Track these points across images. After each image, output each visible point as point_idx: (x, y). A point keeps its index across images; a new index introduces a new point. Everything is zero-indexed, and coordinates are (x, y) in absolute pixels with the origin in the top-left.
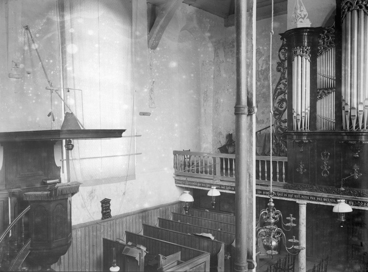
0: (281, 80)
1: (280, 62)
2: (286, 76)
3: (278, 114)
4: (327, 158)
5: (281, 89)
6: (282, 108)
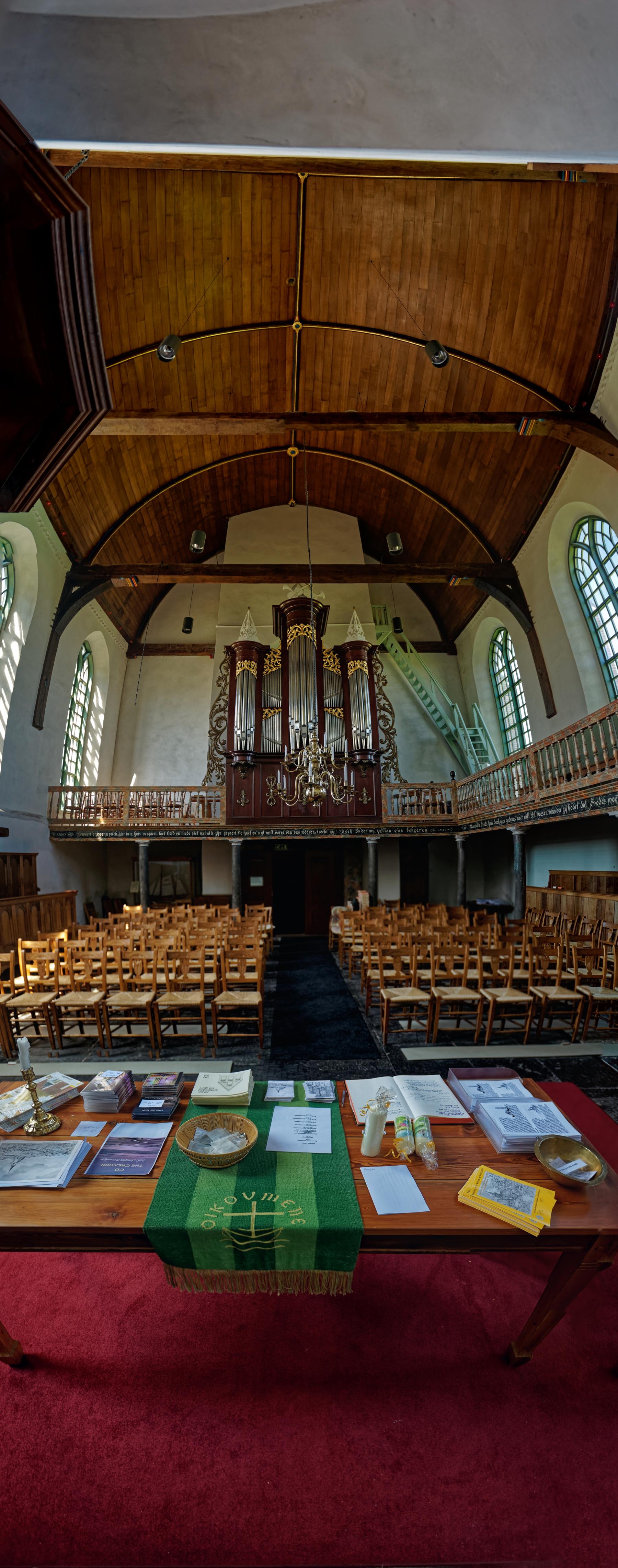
3: (214, 735)
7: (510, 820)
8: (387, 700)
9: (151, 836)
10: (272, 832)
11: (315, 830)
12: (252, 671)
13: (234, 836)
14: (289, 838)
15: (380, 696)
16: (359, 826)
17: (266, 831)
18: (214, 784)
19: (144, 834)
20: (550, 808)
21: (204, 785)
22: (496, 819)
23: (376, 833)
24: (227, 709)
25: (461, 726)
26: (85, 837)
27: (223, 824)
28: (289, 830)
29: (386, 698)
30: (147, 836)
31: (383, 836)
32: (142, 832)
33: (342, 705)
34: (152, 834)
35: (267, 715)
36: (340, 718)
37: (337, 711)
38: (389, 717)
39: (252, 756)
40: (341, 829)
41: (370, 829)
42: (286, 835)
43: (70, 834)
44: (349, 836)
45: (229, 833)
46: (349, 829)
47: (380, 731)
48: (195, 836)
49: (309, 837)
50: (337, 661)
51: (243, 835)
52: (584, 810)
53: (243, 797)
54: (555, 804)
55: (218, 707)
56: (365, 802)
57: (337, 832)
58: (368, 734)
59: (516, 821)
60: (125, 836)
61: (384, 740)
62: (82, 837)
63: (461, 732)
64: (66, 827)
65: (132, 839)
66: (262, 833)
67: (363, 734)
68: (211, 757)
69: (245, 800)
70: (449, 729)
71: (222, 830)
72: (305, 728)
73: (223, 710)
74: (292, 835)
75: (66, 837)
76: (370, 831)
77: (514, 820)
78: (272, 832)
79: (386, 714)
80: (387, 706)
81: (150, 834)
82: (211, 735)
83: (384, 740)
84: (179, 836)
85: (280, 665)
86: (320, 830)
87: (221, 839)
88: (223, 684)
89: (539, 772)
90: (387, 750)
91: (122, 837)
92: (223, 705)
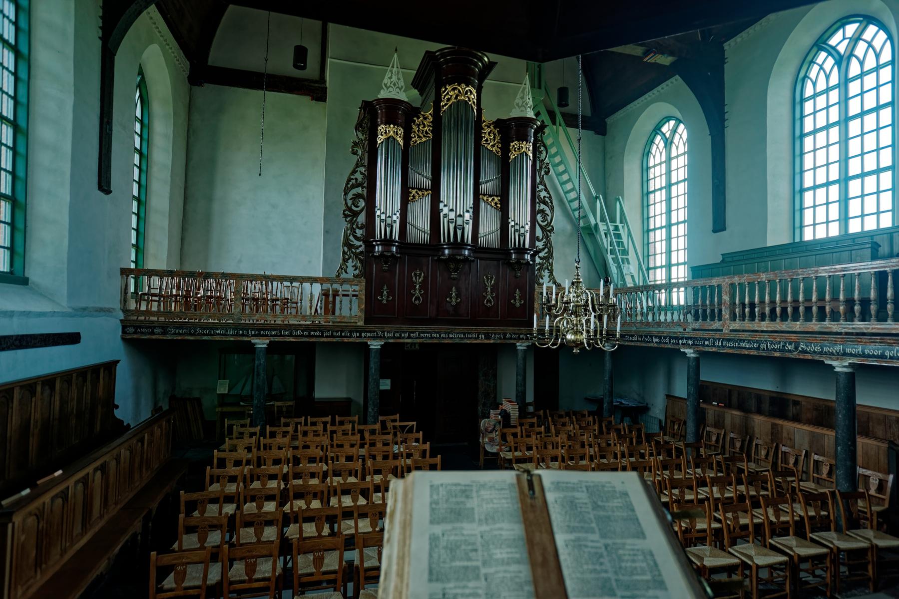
0: (357, 166)
2: (366, 162)
3: (349, 216)
4: (419, 279)
5: (356, 179)
6: (358, 207)
7: (685, 341)
8: (548, 193)
9: (272, 336)
10: (416, 334)
14: (435, 341)
15: (541, 187)
18: (350, 276)
20: (744, 341)
21: (338, 276)
22: (665, 337)
24: (365, 185)
25: (603, 220)
26: (180, 334)
27: (361, 323)
28: (436, 333)
29: (546, 190)
30: (266, 336)
32: (260, 330)
33: (499, 193)
34: (273, 333)
35: (414, 196)
36: (497, 208)
37: (493, 199)
38: (548, 212)
39: (396, 246)
40: (492, 334)
41: (521, 334)
42: (432, 338)
43: (157, 330)
44: (499, 342)
45: (369, 335)
46: (500, 334)
48: (327, 337)
49: (457, 341)
50: (498, 138)
51: (384, 337)
52: (789, 351)
54: (750, 338)
55: (354, 181)
56: (518, 305)
57: (488, 337)
59: (693, 344)
60: (237, 335)
61: (541, 238)
62: (175, 334)
63: (602, 227)
64: (153, 322)
66: (406, 335)
67: (522, 231)
68: (347, 243)
69: (388, 297)
70: (589, 221)
71: (360, 330)
74: (439, 338)
75: (153, 333)
76: (521, 336)
77: (691, 342)
78: (416, 334)
79: (546, 208)
80: (547, 199)
81: (270, 333)
82: (346, 216)
83: (541, 238)
84: (306, 336)
85: (431, 135)
86: (469, 333)
88: (360, 152)
89: (733, 304)
90: (543, 249)
92: (360, 180)
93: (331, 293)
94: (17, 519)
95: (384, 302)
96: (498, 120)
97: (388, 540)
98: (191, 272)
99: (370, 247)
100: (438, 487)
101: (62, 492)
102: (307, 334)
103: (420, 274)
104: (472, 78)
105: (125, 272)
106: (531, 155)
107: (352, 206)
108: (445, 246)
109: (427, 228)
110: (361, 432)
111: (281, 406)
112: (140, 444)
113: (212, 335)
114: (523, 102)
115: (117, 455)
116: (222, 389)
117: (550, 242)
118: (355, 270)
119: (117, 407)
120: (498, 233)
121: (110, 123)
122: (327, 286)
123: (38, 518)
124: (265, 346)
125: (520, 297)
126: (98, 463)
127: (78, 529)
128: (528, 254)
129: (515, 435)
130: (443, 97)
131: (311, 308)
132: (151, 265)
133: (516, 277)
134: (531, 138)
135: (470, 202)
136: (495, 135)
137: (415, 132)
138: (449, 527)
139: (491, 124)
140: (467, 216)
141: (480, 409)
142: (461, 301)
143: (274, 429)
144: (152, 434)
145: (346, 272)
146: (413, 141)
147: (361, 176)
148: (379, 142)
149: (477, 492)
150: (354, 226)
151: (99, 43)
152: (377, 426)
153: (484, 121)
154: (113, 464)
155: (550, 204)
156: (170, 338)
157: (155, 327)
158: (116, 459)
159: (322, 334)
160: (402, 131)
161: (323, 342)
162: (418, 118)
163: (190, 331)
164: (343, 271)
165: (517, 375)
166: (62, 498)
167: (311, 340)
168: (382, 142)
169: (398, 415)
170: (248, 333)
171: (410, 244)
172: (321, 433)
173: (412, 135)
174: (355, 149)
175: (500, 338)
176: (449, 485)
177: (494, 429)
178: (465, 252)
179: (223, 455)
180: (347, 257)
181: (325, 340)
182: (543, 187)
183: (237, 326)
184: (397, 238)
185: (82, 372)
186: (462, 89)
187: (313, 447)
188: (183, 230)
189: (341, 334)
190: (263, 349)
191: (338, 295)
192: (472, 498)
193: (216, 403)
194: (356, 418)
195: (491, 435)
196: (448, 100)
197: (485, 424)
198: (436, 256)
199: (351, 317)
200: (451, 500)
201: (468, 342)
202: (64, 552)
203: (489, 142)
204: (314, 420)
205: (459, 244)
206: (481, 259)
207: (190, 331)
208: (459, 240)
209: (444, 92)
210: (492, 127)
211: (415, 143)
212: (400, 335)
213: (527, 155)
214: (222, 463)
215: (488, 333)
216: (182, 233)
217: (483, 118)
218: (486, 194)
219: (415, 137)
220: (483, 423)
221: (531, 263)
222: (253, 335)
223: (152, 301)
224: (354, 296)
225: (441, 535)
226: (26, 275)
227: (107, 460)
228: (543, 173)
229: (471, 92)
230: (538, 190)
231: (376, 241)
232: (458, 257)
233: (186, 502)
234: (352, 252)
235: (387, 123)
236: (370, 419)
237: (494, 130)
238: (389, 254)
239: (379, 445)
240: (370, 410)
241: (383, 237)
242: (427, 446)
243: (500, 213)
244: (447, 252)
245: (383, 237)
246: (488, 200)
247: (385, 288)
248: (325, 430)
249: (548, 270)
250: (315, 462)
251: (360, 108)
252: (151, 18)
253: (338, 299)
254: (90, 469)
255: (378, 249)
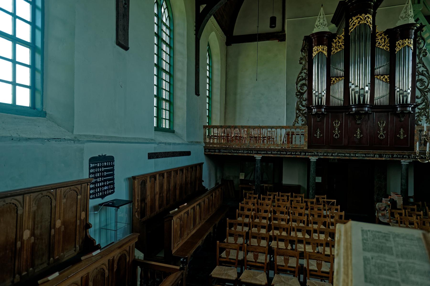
0: (302, 70)
1: (302, 57)
2: (307, 67)
3: (299, 95)
4: (338, 125)
5: (302, 76)
8: (426, 68)
9: (263, 154)
10: (336, 154)
11: (365, 154)
12: (324, 52)
13: (313, 156)
14: (347, 158)
15: (419, 65)
16: (396, 153)
17: (332, 153)
19: (259, 152)
21: (294, 125)
23: (409, 158)
24: (307, 79)
26: (225, 152)
27: (306, 148)
28: (348, 153)
29: (424, 66)
30: (261, 154)
31: (414, 160)
32: (258, 151)
33: (388, 72)
34: (263, 152)
35: (334, 81)
37: (384, 77)
39: (324, 108)
41: (404, 155)
42: (345, 156)
43: (217, 151)
44: (388, 159)
45: (310, 154)
46: (389, 154)
47: (417, 89)
48: (289, 154)
49: (361, 158)
50: (387, 40)
51: (318, 155)
53: (318, 133)
55: (301, 78)
57: (380, 156)
58: (409, 93)
60: (248, 153)
62: (223, 152)
64: (215, 147)
65: (252, 155)
66: (330, 154)
67: (405, 93)
68: (298, 109)
69: (320, 135)
72: (363, 90)
73: (304, 79)
74: (350, 156)
75: (215, 152)
76: (405, 156)
78: (336, 154)
80: (424, 72)
81: (262, 152)
82: (297, 95)
83: (419, 96)
85: (343, 47)
87: (304, 157)
88: (304, 63)
90: (421, 103)
91: (246, 153)
92: (304, 76)
93: (290, 133)
94: (174, 218)
95: (318, 137)
96: (387, 30)
97: (338, 255)
98: (229, 126)
99: (310, 109)
100: (366, 231)
101: (187, 211)
102: (279, 153)
103: (338, 122)
104: (369, 9)
105: (205, 127)
106: (412, 46)
107: (301, 90)
108: (353, 106)
109: (342, 97)
110: (306, 202)
111: (267, 186)
112: (211, 197)
113: (238, 153)
114: (406, 15)
115: (204, 200)
116: (242, 177)
117: (427, 99)
118: (302, 122)
119: (203, 181)
120: (388, 96)
121: (198, 68)
122: (288, 130)
123: (180, 220)
124: (260, 158)
125: (403, 133)
126: (198, 202)
127: (192, 227)
128: (410, 107)
129: (401, 214)
130: (350, 24)
131: (281, 141)
132: (214, 123)
133: (400, 121)
134: (412, 35)
135: (368, 80)
136: (385, 39)
137: (334, 47)
138: (376, 255)
139: (382, 34)
140: (367, 88)
141: (375, 197)
142: (363, 136)
143: (264, 196)
144: (216, 193)
145: (298, 123)
146: (333, 52)
147: (305, 75)
148: (314, 55)
149: (394, 238)
150: (301, 100)
151: (195, 36)
152: (315, 200)
153: (378, 33)
154: (203, 203)
155: (427, 75)
156: (221, 154)
157: (216, 149)
158: (203, 202)
159: (286, 153)
160: (326, 47)
161: (287, 157)
162: (336, 39)
163: (229, 151)
164: (296, 122)
165: (401, 179)
166: (187, 214)
167: (281, 156)
168: (316, 55)
169: (326, 196)
170: (253, 152)
171: (332, 107)
172: (286, 200)
173: (332, 49)
174: (301, 61)
175: (389, 157)
176: (374, 231)
177: (385, 209)
178: (365, 109)
179: (243, 205)
180: (298, 115)
181: (288, 156)
182: (421, 65)
183: (248, 149)
184: (325, 104)
185: (192, 167)
186: (363, 17)
187: (282, 207)
188: (226, 108)
189: (296, 153)
190: (259, 160)
191: (294, 135)
192: (390, 241)
193: (239, 183)
194: (303, 195)
195: (383, 212)
196: (354, 25)
197: (379, 206)
198: (347, 112)
199: (300, 145)
200: (376, 240)
201: (368, 159)
202: (188, 234)
203: (381, 44)
204: (283, 194)
205: (362, 104)
206: (376, 112)
207: (229, 151)
208: (362, 102)
209: (351, 21)
210: (383, 35)
211: (334, 53)
212: (327, 154)
213: (408, 47)
214: (243, 209)
215: (381, 154)
216: (225, 110)
217: (377, 31)
218: (379, 75)
219: (334, 49)
220: (378, 205)
221: (412, 112)
222: (255, 153)
223: (215, 138)
224: (302, 134)
225: (370, 258)
226: (174, 130)
227: (201, 202)
228: (421, 56)
229: (368, 17)
230: (417, 67)
231: (313, 107)
232: (361, 112)
233: (229, 223)
234: (301, 113)
235: (318, 45)
236: (310, 196)
237: (384, 36)
238: (320, 113)
239: (316, 210)
240: (311, 192)
241: (317, 104)
242: (343, 213)
243: (389, 85)
244: (354, 109)
245: (317, 104)
246: (380, 78)
247: (318, 130)
248: (288, 199)
249: (425, 116)
250: (283, 214)
251: (303, 40)
252: (212, 21)
253: (294, 136)
254: (195, 204)
255: (315, 110)
